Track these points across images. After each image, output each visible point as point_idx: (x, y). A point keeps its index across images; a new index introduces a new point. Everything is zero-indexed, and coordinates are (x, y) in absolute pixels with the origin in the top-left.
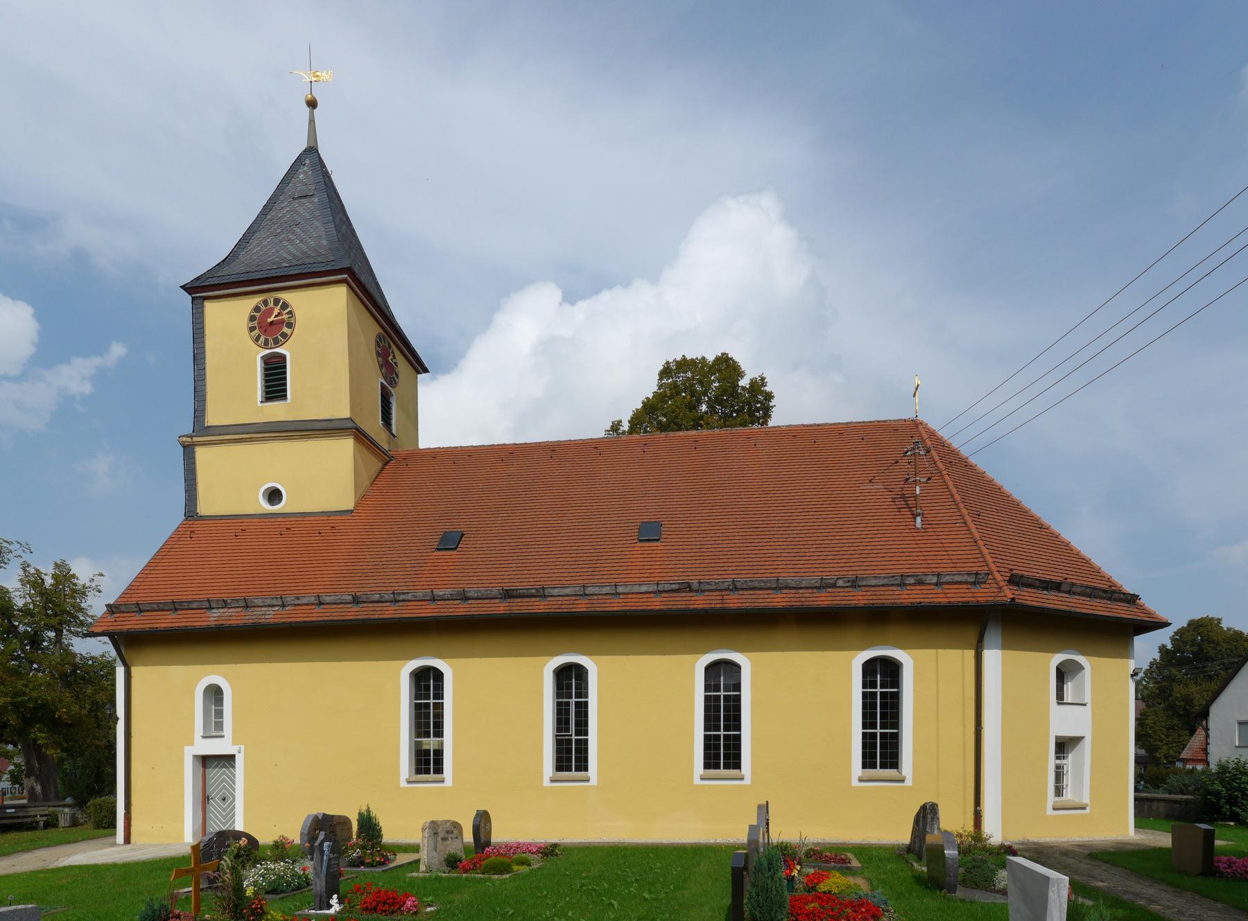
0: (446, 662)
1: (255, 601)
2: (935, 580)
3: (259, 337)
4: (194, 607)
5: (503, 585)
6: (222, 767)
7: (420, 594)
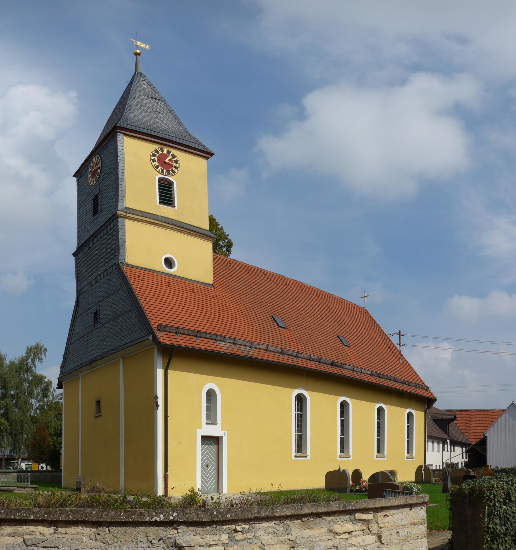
0: (308, 394)
1: (239, 341)
2: (359, 370)
3: (157, 167)
4: (207, 337)
5: (333, 359)
6: (206, 444)
7: (306, 355)
